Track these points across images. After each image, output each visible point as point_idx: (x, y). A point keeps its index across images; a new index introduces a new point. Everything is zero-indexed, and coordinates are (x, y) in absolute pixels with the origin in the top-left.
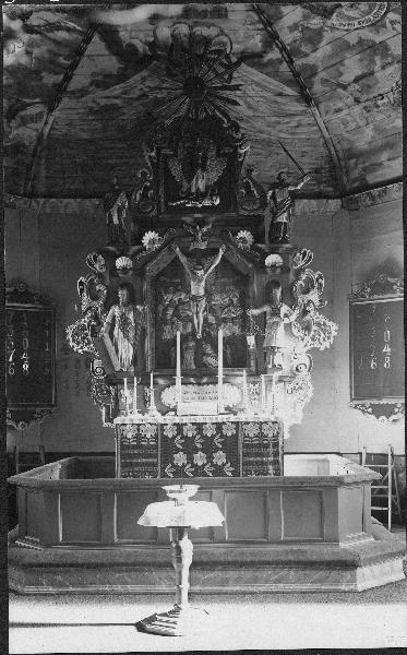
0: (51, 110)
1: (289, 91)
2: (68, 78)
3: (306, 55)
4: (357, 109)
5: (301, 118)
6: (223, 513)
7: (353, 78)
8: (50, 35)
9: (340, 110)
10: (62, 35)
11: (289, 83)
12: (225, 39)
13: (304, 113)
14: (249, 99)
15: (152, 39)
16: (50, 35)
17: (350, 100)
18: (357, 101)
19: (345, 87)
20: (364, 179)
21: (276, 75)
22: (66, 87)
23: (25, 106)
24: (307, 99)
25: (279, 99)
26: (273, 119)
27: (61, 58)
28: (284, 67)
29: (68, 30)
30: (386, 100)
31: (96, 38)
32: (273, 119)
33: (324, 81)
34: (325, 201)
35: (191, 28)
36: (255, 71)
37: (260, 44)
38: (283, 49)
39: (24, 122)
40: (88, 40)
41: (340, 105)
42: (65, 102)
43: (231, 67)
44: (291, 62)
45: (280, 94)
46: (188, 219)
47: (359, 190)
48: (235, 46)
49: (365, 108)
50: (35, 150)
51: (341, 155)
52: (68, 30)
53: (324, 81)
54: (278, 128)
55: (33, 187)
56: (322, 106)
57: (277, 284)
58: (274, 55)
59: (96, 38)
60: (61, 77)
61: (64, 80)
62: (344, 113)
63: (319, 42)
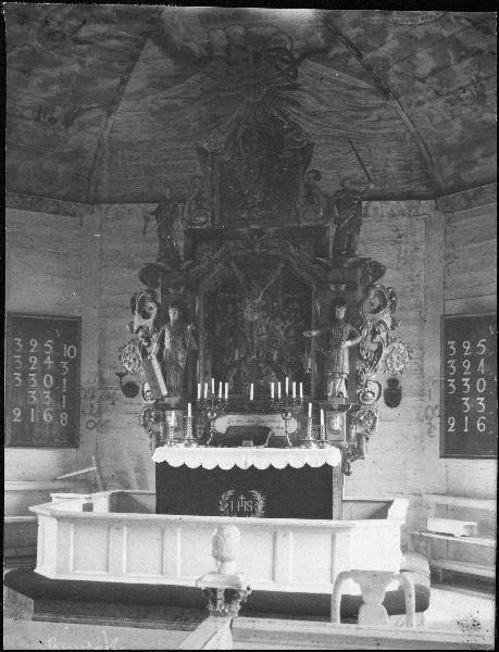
0: (110, 113)
1: (363, 84)
2: (124, 82)
3: (375, 49)
4: (440, 102)
5: (381, 111)
6: (348, 528)
7: (429, 71)
8: (102, 44)
9: (420, 104)
10: (114, 42)
11: (361, 76)
12: (284, 37)
13: (384, 106)
14: (320, 95)
15: (206, 41)
16: (102, 44)
17: (431, 93)
18: (438, 94)
19: (422, 80)
20: (459, 178)
21: (345, 68)
22: (123, 91)
23: (81, 112)
24: (385, 92)
25: (351, 92)
26: (349, 114)
27: (116, 64)
28: (353, 60)
29: (119, 38)
30: (468, 93)
31: (149, 43)
32: (349, 114)
33: (398, 75)
34: (415, 202)
35: (245, 29)
36: (324, 67)
37: (322, 41)
38: (349, 43)
39: (82, 127)
40: (141, 46)
41: (421, 97)
42: (124, 104)
43: (295, 63)
44: (360, 56)
45: (354, 88)
46: (244, 230)
47: (453, 190)
48: (296, 43)
49: (448, 101)
50: (96, 154)
51: (432, 151)
52: (119, 38)
53: (398, 75)
54: (358, 122)
55: (96, 191)
56: (402, 99)
57: (341, 303)
58: (340, 49)
59: (149, 43)
60: (117, 81)
61: (122, 83)
62: (426, 106)
63: (386, 36)
